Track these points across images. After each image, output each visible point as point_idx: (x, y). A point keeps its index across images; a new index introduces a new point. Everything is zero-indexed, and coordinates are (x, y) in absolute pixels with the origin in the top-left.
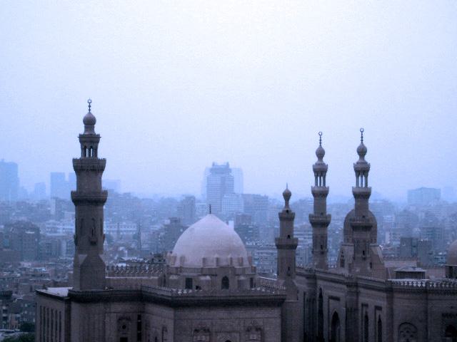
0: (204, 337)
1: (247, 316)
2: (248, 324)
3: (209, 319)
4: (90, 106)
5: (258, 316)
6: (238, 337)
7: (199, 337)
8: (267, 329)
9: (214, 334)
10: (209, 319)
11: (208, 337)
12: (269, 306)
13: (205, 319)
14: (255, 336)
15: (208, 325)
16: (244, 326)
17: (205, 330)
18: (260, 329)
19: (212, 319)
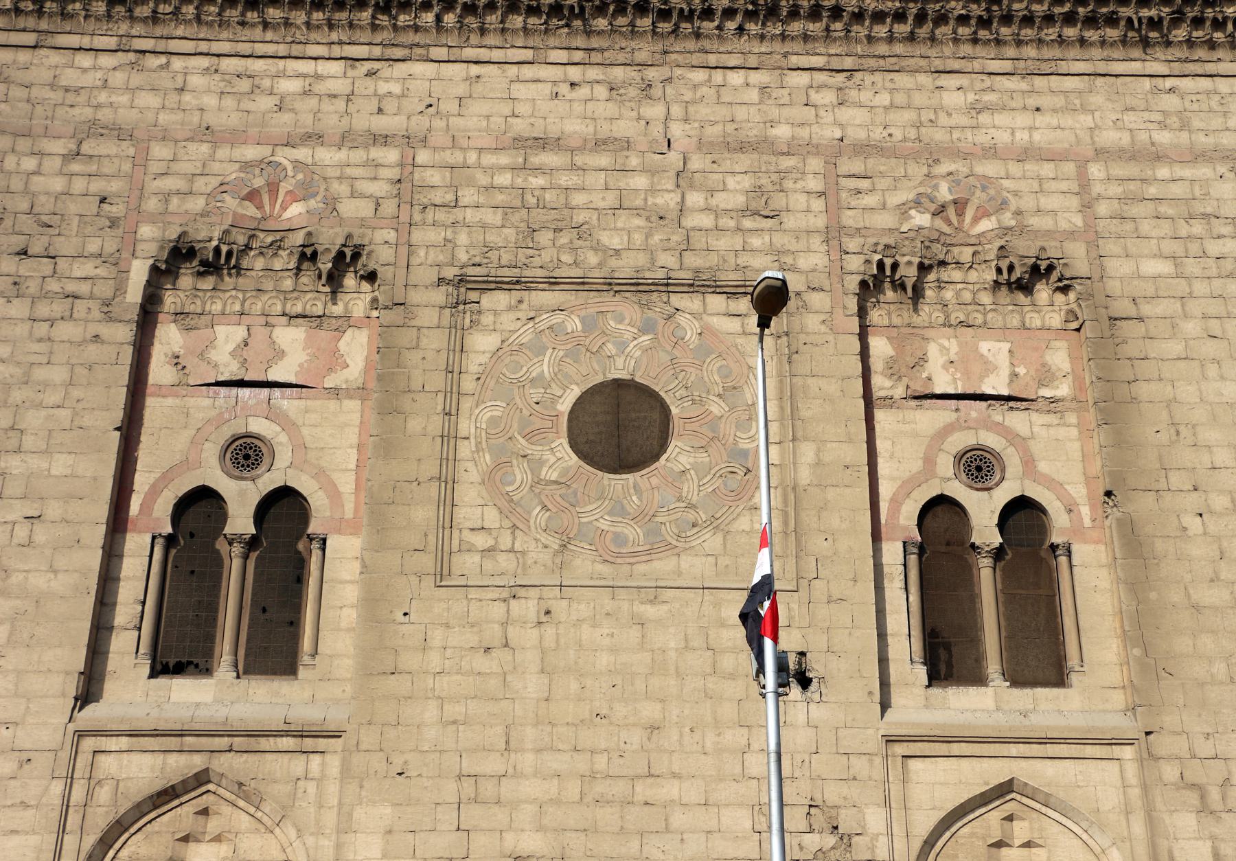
0: (291, 337)
1: (856, 122)
2: (888, 211)
3: (384, 139)
5: (1011, 127)
7: (228, 336)
8: (1135, 269)
9: (429, 303)
10: (384, 139)
11: (356, 348)
13: (314, 138)
14: (995, 350)
15: (355, 200)
16: (834, 234)
17: (308, 256)
18: (1039, 272)
19: (409, 140)
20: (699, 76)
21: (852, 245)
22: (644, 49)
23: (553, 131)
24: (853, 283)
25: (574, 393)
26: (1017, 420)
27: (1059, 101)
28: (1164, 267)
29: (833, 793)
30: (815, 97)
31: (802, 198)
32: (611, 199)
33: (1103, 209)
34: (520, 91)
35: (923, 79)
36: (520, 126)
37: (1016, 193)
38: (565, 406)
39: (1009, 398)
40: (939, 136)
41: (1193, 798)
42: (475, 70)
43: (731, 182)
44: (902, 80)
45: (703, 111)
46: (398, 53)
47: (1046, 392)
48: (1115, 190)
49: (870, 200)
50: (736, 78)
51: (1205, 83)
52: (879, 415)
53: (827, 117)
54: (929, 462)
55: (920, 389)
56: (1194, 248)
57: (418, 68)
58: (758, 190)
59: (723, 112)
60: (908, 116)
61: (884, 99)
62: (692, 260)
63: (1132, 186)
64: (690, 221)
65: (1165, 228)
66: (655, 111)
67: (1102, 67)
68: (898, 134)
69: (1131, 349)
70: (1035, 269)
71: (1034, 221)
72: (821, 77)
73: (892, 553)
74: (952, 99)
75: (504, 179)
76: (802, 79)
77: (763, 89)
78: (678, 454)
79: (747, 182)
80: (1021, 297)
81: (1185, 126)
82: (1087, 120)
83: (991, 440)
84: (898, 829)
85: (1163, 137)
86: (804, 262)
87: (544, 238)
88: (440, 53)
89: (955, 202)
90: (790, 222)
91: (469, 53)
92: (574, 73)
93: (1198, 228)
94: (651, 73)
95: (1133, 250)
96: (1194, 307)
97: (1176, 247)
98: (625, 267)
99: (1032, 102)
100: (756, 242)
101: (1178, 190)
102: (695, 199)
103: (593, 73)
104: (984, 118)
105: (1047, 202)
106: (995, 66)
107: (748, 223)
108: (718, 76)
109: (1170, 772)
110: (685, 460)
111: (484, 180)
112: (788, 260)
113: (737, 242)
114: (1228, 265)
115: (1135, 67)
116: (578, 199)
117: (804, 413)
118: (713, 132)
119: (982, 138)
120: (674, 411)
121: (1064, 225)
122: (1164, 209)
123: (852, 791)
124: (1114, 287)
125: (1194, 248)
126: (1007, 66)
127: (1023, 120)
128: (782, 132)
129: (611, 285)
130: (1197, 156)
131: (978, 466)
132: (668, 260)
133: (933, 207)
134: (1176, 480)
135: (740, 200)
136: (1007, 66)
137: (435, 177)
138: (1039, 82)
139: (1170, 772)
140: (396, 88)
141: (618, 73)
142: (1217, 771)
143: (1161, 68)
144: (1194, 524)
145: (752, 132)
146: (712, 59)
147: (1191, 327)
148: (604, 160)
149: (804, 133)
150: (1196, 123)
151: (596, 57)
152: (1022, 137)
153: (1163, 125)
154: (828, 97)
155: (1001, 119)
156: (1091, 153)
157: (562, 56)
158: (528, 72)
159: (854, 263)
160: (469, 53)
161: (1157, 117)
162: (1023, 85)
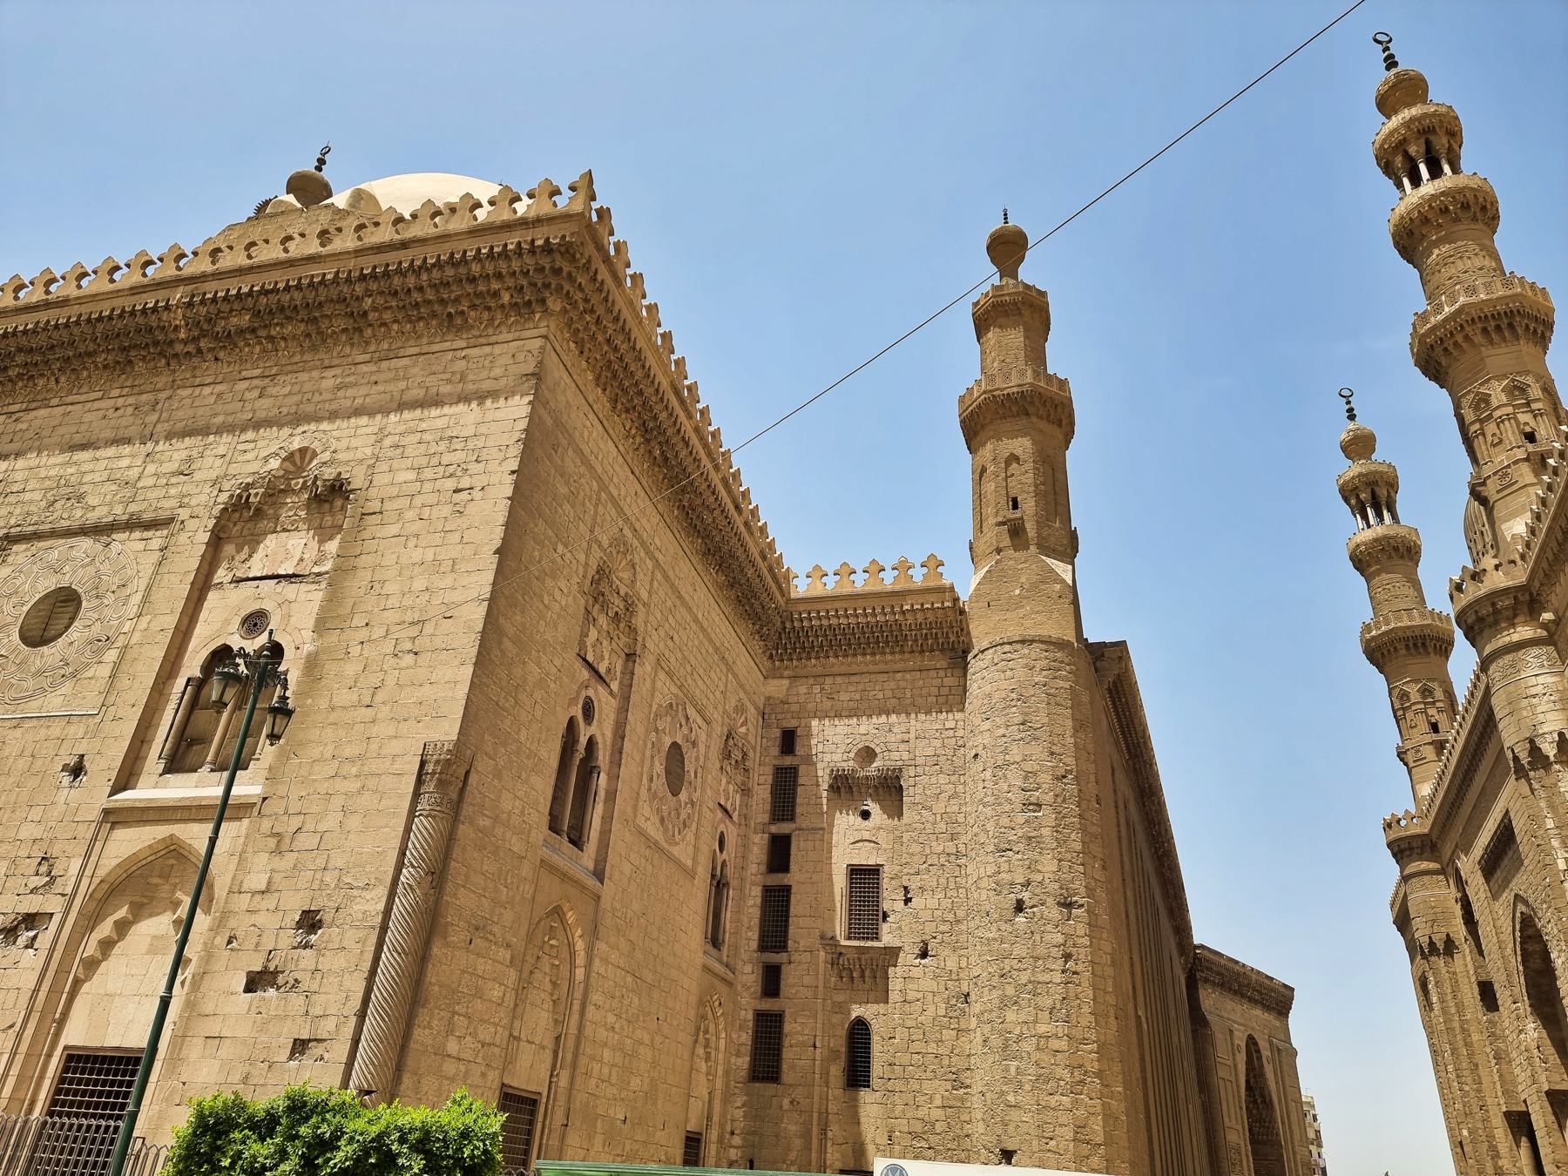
4: (321, 162)
6: (147, 569)
12: (452, 323)
20: (188, 392)
21: (226, 486)
22: (162, 380)
23: (94, 438)
24: (216, 511)
25: (38, 596)
26: (290, 590)
27: (391, 375)
28: (411, 476)
29: (55, 851)
30: (248, 395)
31: (211, 460)
32: (105, 475)
33: (387, 442)
34: (88, 417)
35: (315, 374)
36: (78, 439)
37: (338, 439)
38: (26, 609)
39: (294, 576)
40: (309, 408)
41: (272, 842)
42: (70, 408)
43: (176, 456)
44: (303, 376)
45: (180, 413)
46: (34, 405)
47: (316, 570)
48: (401, 428)
49: (249, 456)
50: (207, 390)
51: (487, 349)
52: (212, 596)
53: (248, 406)
54: (227, 622)
55: (240, 574)
56: (435, 461)
57: (42, 412)
58: (190, 459)
59: (191, 412)
60: (297, 398)
61: (287, 389)
62: (133, 508)
63: (412, 424)
64: (140, 485)
65: (423, 448)
66: (153, 417)
67: (425, 349)
68: (285, 410)
69: (366, 534)
70: (333, 486)
71: (340, 456)
72: (256, 382)
73: (180, 683)
74: (328, 383)
75: (52, 473)
76: (244, 385)
77: (219, 395)
78: (76, 633)
79: (184, 454)
80: (327, 506)
81: (462, 379)
82: (402, 385)
83: (267, 605)
84: (88, 872)
85: (446, 389)
86: (193, 503)
87: (58, 505)
88: (55, 401)
89: (300, 450)
90: (198, 476)
91: (70, 399)
92: (120, 402)
93: (443, 446)
94: (163, 395)
95: (395, 466)
96: (418, 501)
97: (424, 461)
98: (93, 517)
99: (374, 378)
100: (173, 491)
101: (441, 423)
102: (151, 468)
103: (131, 400)
104: (341, 393)
105: (354, 443)
106: (361, 358)
107: (173, 480)
108: (197, 391)
109: (266, 825)
110: (76, 635)
111: (43, 473)
112: (186, 500)
113: (161, 493)
114: (451, 469)
115: (447, 345)
116: (87, 478)
117: (152, 598)
118: (180, 426)
119: (334, 406)
120: (84, 604)
121: (359, 455)
122: (427, 437)
123: (69, 848)
124: (373, 492)
125: (435, 461)
126: (367, 357)
127: (363, 391)
128: (219, 420)
129: (83, 531)
130: (464, 398)
131: (254, 622)
132: (118, 510)
133: (284, 454)
134: (358, 621)
135: (173, 466)
136: (367, 357)
137: (19, 476)
138: (384, 364)
139: (266, 825)
140: (24, 426)
141: (144, 397)
142: (295, 822)
143: (464, 344)
144: (355, 650)
145: (201, 423)
146: (198, 381)
147: (410, 515)
148: (112, 451)
149: (230, 419)
150: (471, 377)
151: (136, 390)
152: (359, 401)
153: (449, 381)
154: (256, 393)
155: (350, 392)
156: (395, 406)
157: (116, 392)
158: (96, 405)
159: (224, 497)
160: (70, 399)
161: (447, 376)
162: (374, 368)
